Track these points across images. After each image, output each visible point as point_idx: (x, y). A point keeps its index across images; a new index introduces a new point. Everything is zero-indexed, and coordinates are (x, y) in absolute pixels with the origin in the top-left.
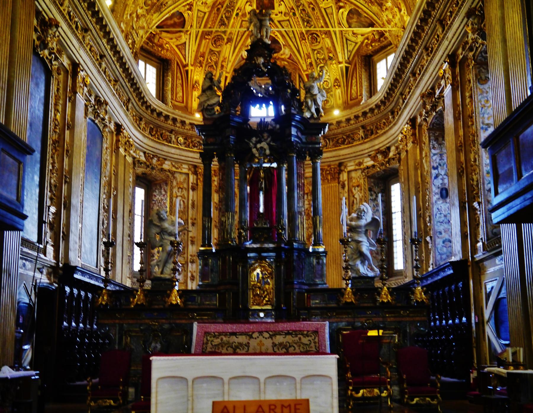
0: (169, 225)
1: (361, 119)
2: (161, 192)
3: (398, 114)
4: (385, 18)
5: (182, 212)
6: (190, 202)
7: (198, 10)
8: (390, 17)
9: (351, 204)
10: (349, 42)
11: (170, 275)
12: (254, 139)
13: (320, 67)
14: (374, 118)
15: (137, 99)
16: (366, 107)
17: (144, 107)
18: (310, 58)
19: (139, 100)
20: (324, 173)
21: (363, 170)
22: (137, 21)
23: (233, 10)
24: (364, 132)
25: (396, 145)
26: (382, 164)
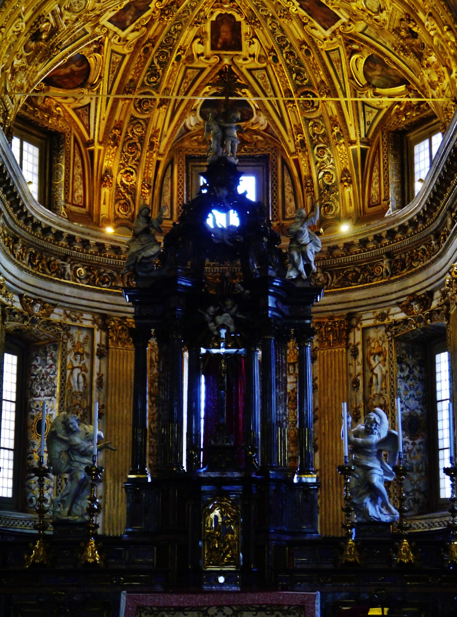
0: (82, 440)
1: (387, 241)
2: (45, 360)
3: (445, 240)
4: (426, 78)
5: (81, 395)
6: (95, 377)
7: (113, 51)
8: (435, 79)
9: (367, 384)
10: (367, 109)
11: (82, 516)
12: (212, 309)
13: (318, 149)
14: (407, 242)
15: (11, 210)
16: (393, 223)
17: (22, 221)
18: (302, 133)
19: (15, 211)
20: (323, 330)
21: (388, 328)
22: (12, 79)
23: (172, 51)
24: (390, 262)
25: (442, 289)
26: (420, 320)
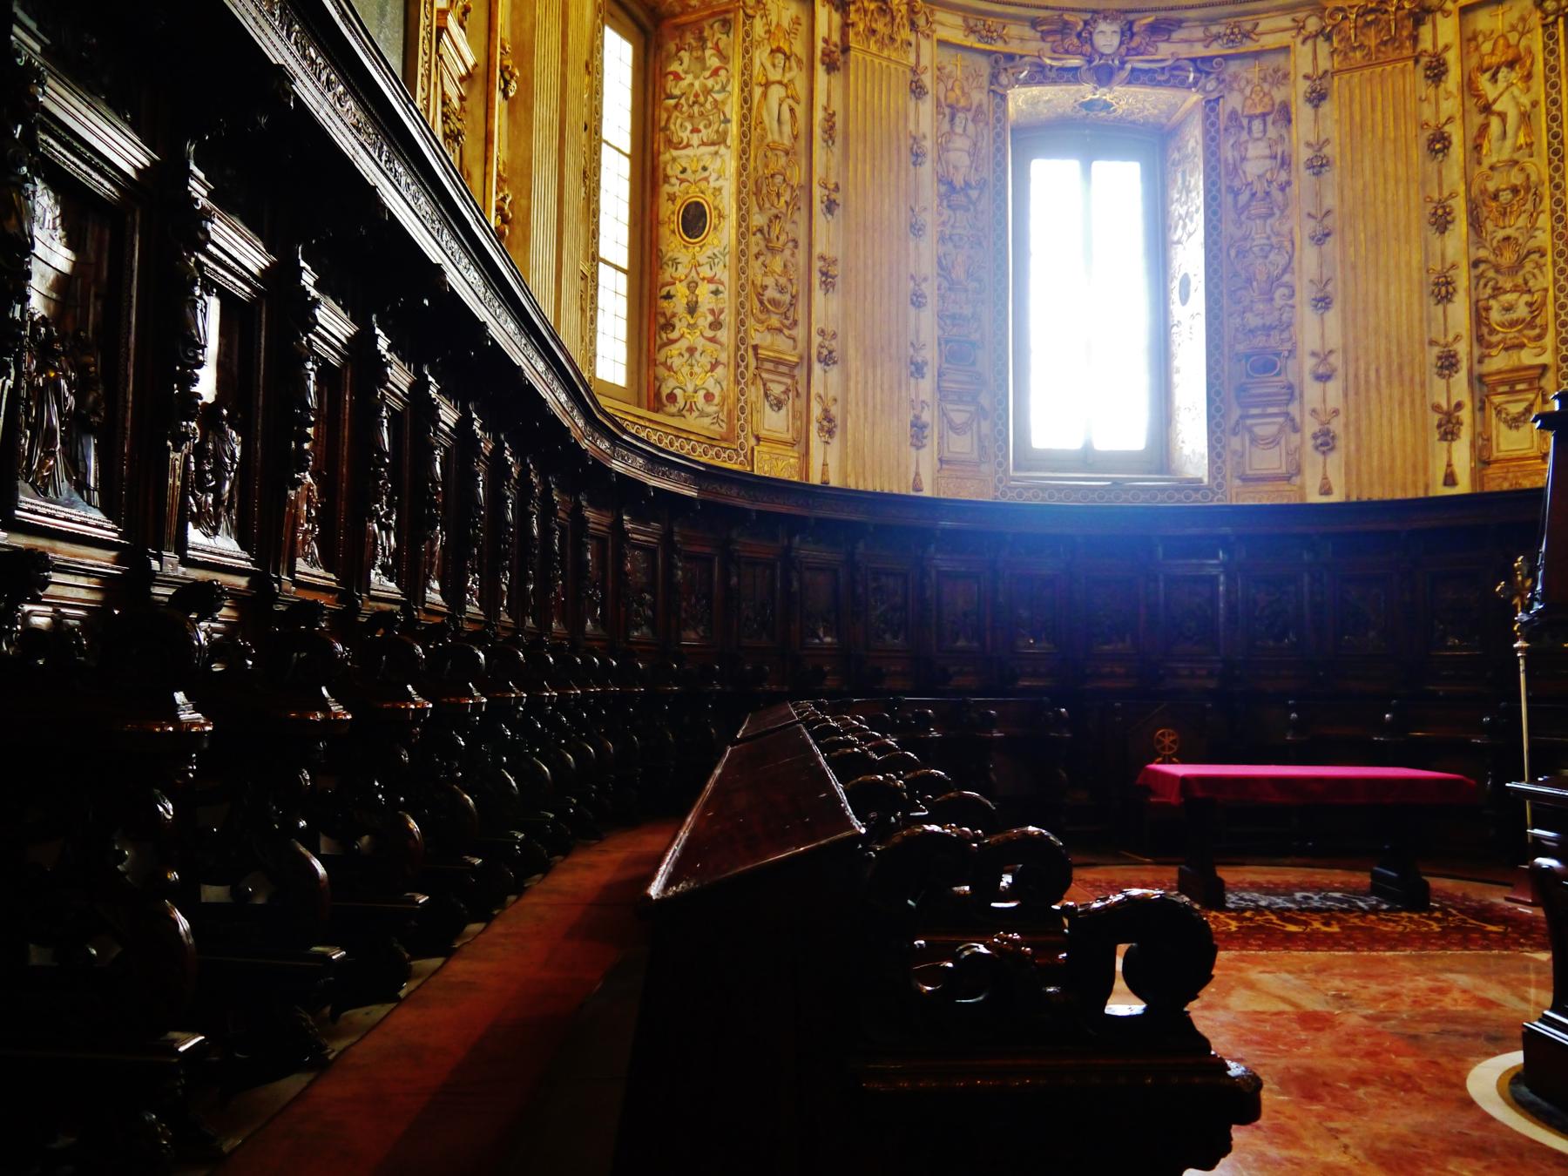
2: (701, 60)
6: (819, 115)
